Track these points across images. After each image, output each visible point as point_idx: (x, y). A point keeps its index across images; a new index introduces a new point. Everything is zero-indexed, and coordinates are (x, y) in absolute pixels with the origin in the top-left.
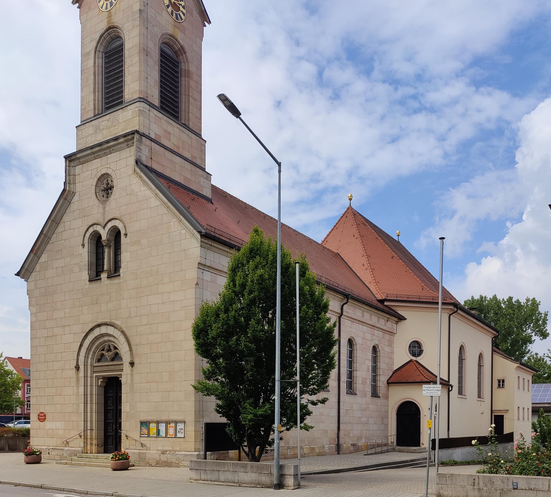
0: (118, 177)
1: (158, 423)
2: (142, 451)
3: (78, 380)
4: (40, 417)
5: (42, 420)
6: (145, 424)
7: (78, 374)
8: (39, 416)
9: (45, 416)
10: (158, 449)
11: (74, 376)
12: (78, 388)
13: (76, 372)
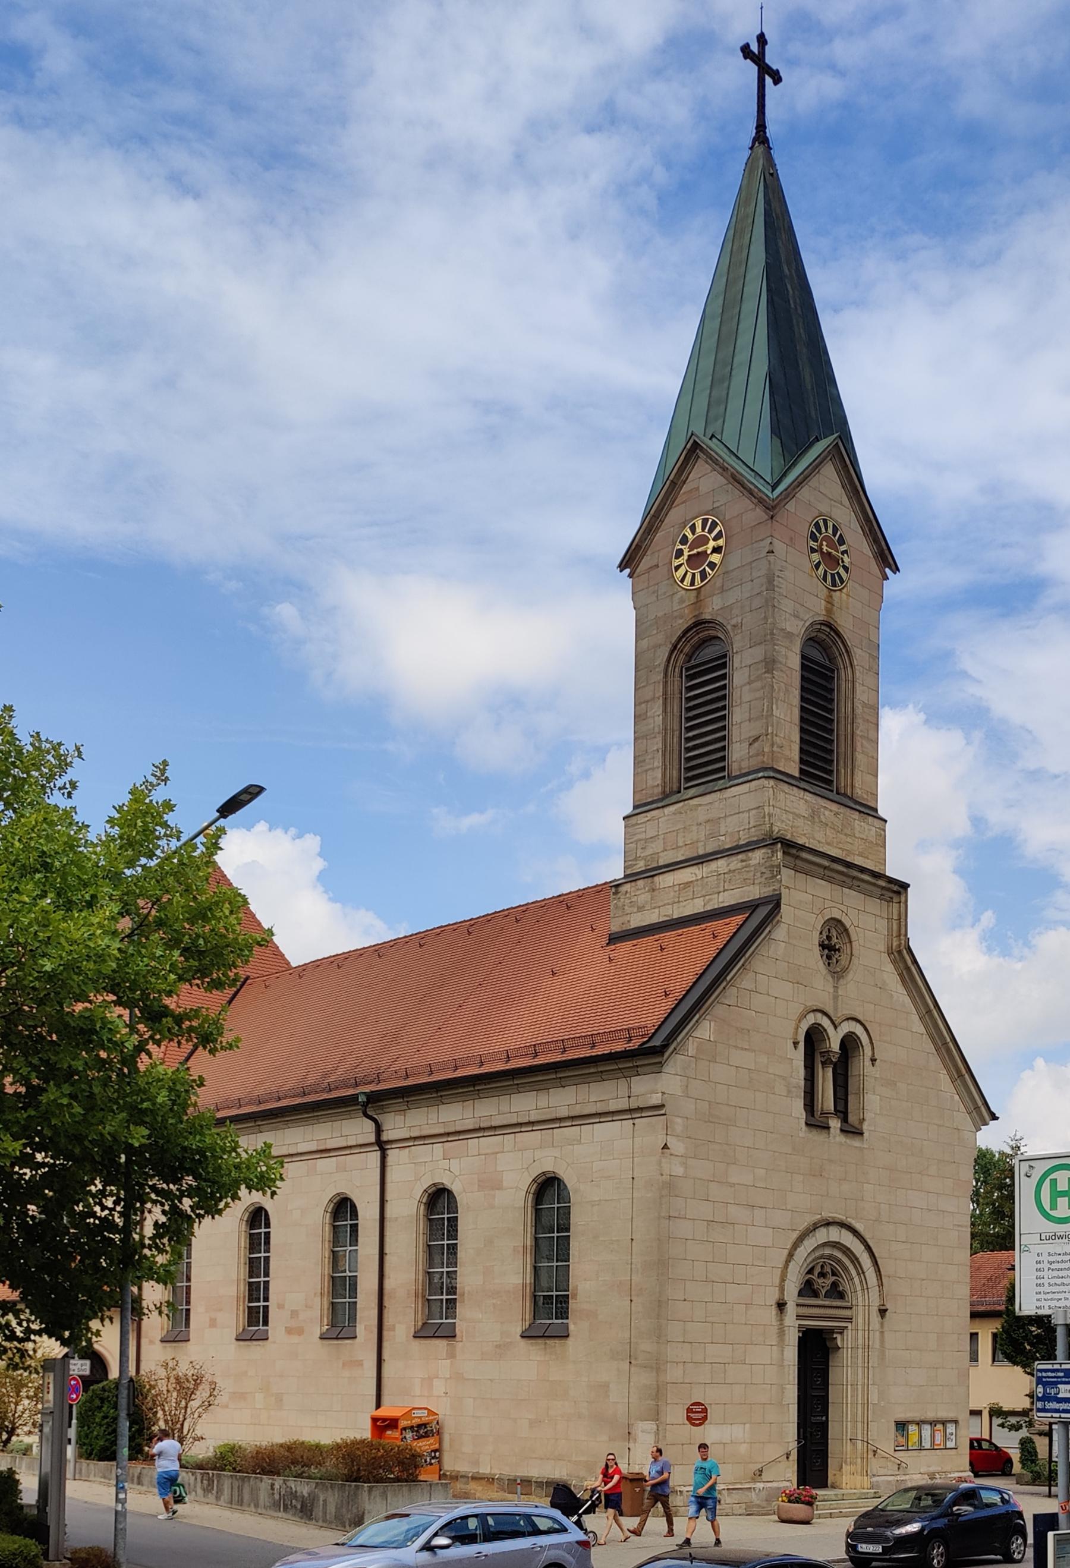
0: (861, 941)
1: (919, 1423)
2: (898, 1478)
3: (781, 1332)
4: (692, 1415)
5: (697, 1422)
6: (901, 1426)
7: (781, 1320)
8: (689, 1410)
9: (705, 1410)
10: (922, 1471)
11: (774, 1324)
12: (783, 1351)
13: (777, 1314)
